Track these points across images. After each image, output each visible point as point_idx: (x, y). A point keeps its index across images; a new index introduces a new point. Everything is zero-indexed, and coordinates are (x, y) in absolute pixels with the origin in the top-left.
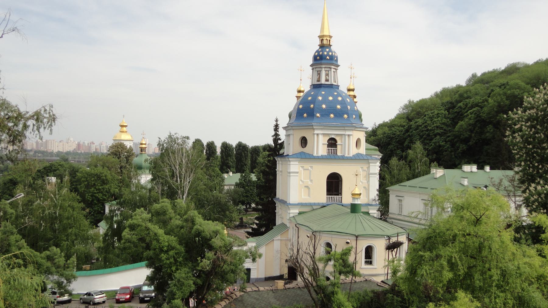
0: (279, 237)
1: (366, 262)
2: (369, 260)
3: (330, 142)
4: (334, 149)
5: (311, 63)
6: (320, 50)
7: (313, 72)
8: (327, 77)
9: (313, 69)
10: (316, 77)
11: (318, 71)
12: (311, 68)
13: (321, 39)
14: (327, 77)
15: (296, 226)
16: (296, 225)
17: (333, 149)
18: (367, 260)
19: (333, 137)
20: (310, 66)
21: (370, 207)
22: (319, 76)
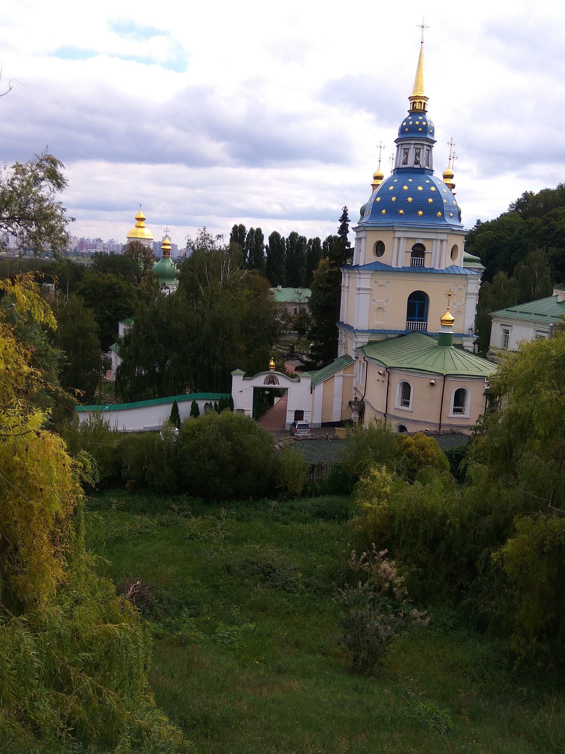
0: (342, 373)
1: (455, 411)
2: (459, 407)
3: (416, 249)
4: (421, 258)
5: (396, 136)
6: (410, 118)
7: (398, 150)
8: (417, 157)
9: (398, 146)
10: (403, 158)
11: (405, 149)
12: (396, 144)
13: (413, 101)
14: (417, 157)
15: (364, 360)
16: (364, 358)
17: (418, 258)
18: (457, 407)
19: (420, 242)
20: (394, 141)
21: (464, 338)
22: (406, 156)
